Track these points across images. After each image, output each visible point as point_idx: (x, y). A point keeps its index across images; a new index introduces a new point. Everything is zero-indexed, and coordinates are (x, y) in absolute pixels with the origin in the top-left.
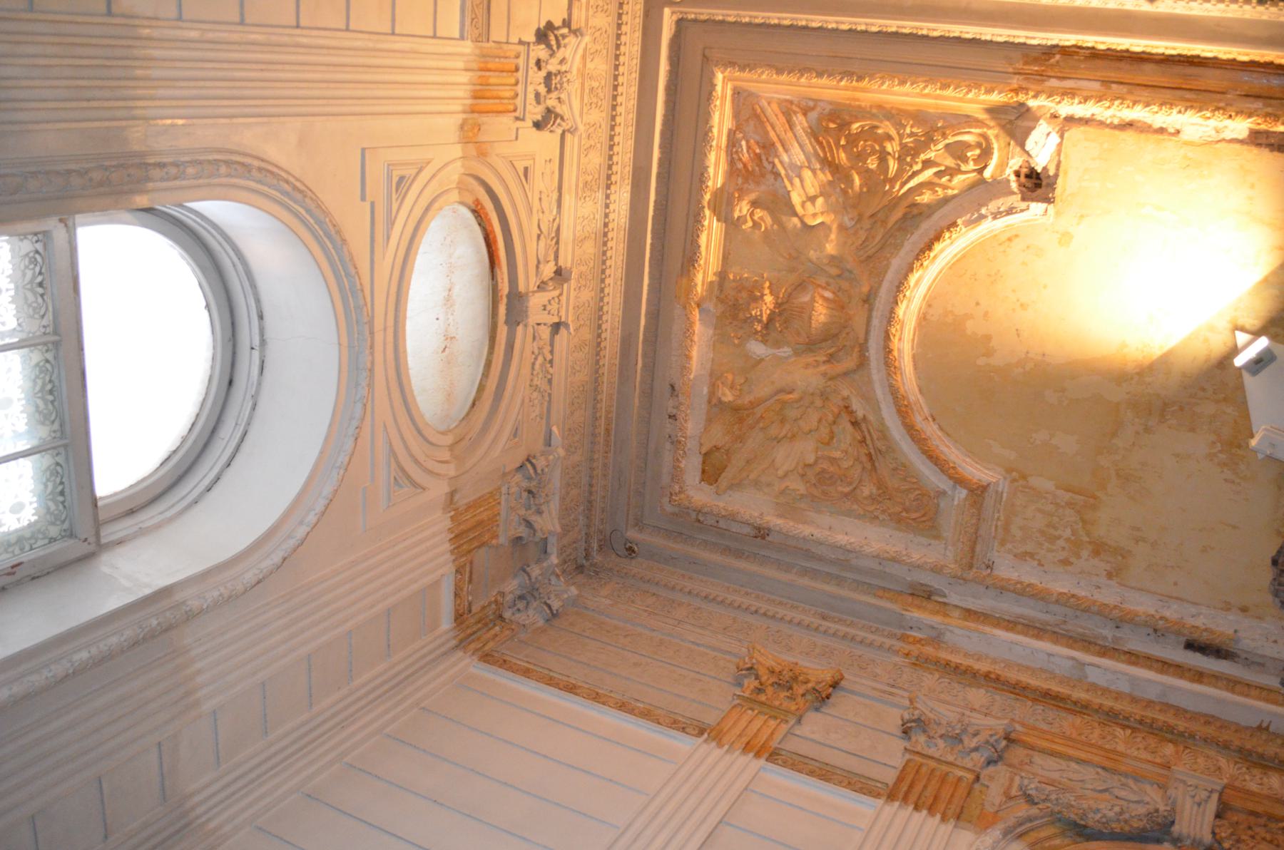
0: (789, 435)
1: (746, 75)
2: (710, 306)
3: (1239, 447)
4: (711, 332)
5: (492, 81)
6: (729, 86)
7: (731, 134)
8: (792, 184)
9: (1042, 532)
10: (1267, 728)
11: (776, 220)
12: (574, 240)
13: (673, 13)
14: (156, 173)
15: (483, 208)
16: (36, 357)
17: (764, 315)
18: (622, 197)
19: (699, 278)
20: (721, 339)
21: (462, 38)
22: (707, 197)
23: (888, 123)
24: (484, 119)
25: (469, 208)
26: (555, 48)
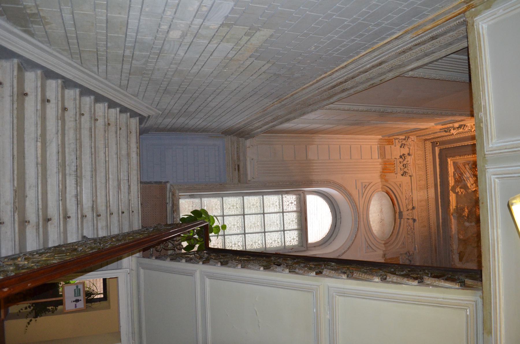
1: (454, 158)
2: (455, 215)
4: (456, 221)
5: (388, 166)
6: (452, 162)
7: (454, 172)
8: (467, 181)
11: (466, 191)
12: (417, 201)
13: (438, 148)
14: (314, 182)
15: (389, 192)
16: (298, 214)
18: (432, 192)
19: (451, 207)
20: (459, 223)
21: (378, 158)
22: (450, 188)
24: (386, 174)
26: (404, 159)
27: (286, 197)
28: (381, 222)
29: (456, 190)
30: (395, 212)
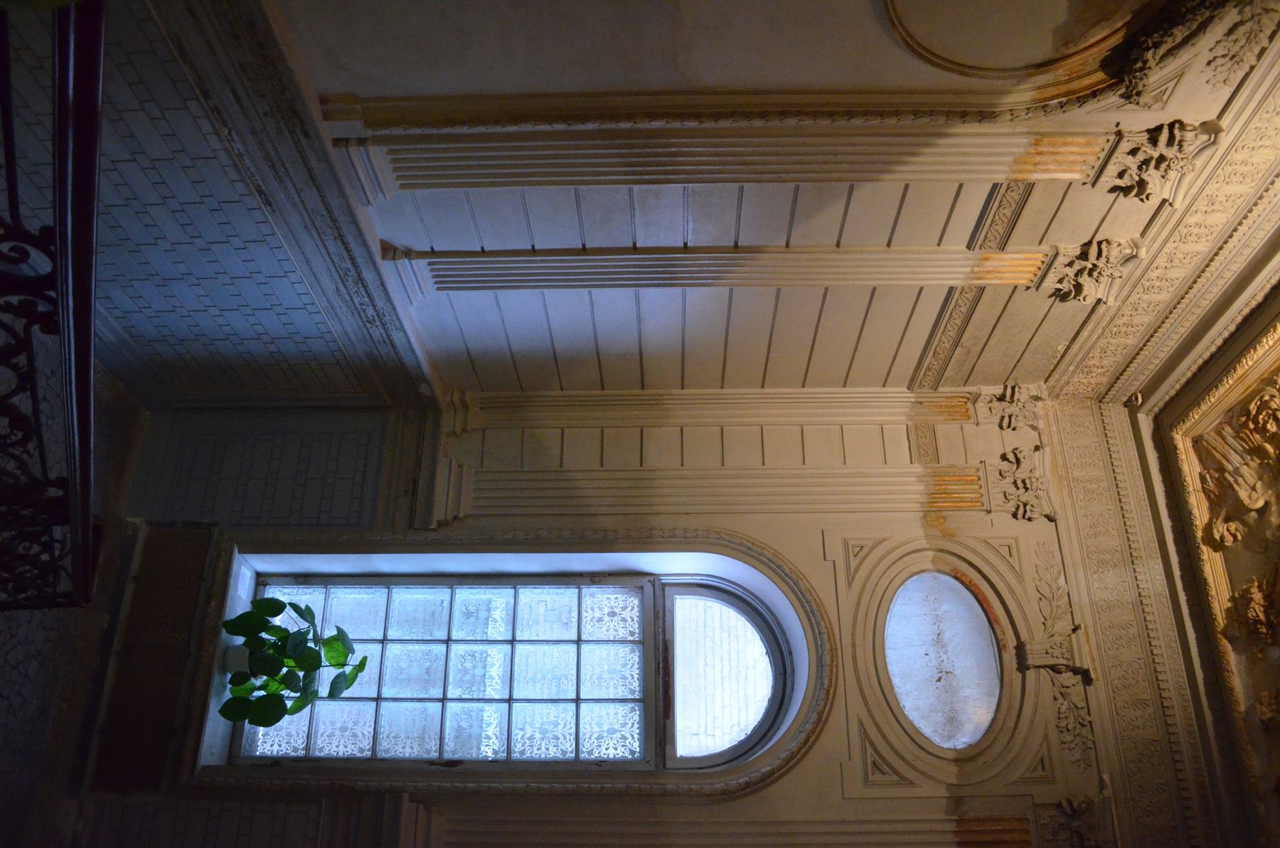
1: (1188, 424)
4: (1244, 657)
7: (1200, 474)
8: (1239, 485)
15: (963, 574)
17: (1260, 614)
23: (1269, 388)
24: (944, 514)
25: (950, 575)
27: (593, 595)
28: (939, 680)
29: (1215, 531)
30: (1000, 647)
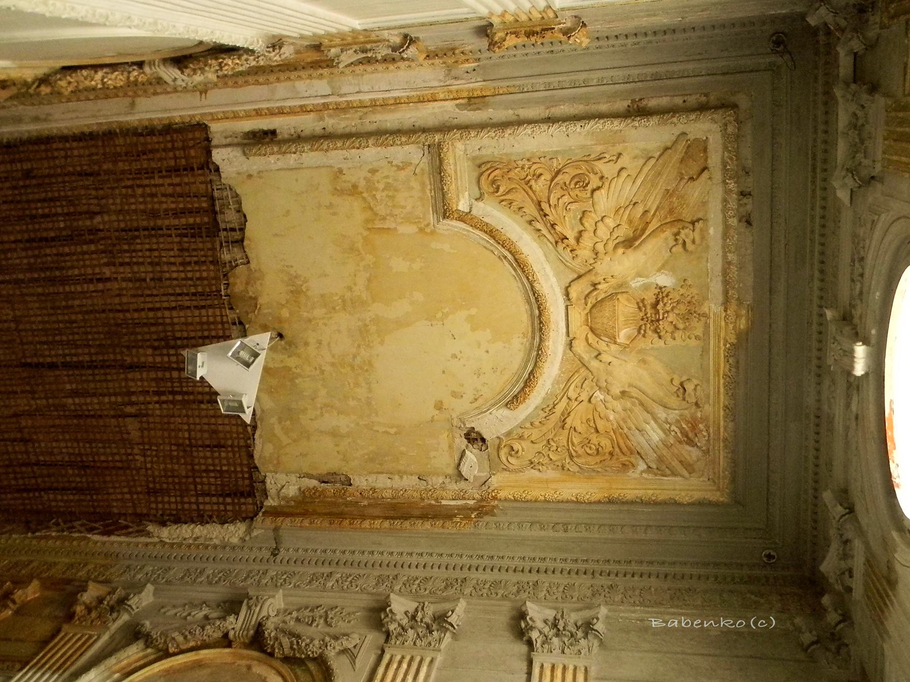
0: (621, 211)
3: (292, 292)
9: (396, 190)
10: (201, 94)
